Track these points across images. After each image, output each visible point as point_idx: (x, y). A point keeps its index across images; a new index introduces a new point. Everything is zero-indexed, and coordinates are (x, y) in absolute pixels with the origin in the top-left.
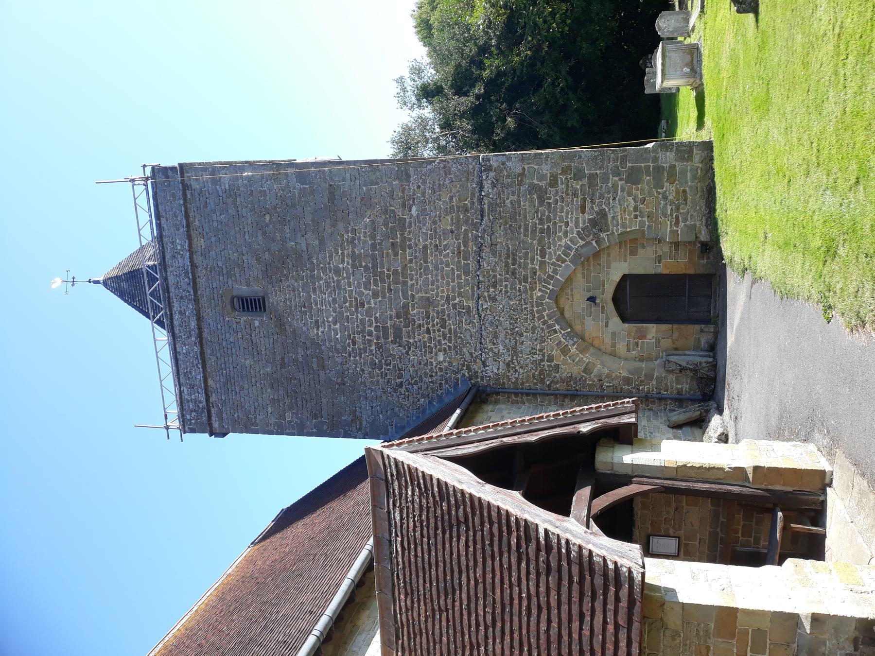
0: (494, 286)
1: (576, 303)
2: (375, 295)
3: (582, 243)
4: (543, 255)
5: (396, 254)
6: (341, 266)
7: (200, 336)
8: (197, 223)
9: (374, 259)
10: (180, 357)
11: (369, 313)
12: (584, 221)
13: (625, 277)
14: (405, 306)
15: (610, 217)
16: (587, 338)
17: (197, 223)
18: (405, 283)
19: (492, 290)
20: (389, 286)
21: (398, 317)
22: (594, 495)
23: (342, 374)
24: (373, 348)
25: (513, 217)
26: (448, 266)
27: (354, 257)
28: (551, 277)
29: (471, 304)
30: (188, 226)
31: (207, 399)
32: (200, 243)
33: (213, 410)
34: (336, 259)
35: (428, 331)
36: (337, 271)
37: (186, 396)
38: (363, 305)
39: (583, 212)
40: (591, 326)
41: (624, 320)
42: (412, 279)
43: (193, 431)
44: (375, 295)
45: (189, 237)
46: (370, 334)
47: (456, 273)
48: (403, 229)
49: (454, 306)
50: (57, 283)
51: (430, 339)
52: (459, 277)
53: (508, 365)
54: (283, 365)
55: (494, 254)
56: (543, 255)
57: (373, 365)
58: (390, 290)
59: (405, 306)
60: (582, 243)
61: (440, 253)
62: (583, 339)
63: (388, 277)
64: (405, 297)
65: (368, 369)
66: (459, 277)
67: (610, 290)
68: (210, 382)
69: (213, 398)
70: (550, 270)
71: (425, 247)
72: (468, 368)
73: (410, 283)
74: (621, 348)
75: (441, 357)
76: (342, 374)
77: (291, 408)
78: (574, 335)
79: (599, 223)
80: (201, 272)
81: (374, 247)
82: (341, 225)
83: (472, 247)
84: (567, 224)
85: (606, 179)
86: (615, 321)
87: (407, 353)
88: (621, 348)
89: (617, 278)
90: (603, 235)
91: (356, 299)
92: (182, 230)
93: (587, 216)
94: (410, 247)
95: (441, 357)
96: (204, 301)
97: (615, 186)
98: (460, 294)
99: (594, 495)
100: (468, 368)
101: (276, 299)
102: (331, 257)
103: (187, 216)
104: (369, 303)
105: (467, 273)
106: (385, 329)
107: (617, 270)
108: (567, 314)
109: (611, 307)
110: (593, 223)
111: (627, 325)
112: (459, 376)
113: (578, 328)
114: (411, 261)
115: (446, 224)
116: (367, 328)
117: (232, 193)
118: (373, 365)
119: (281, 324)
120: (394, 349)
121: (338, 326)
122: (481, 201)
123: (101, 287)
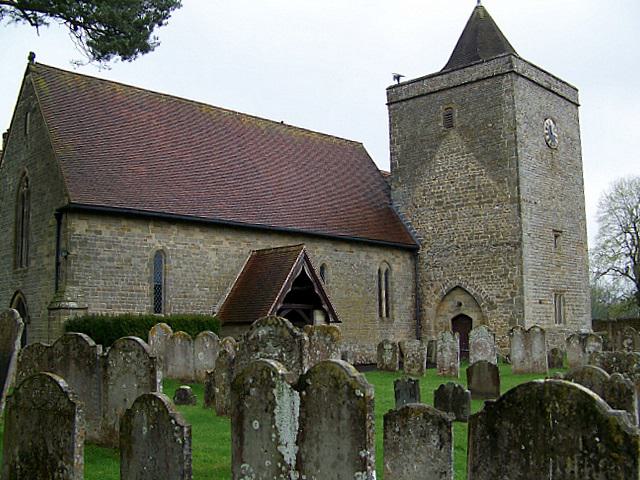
0: (464, 255)
1: (459, 297)
2: (457, 189)
4: (478, 278)
7: (432, 93)
9: (474, 187)
10: (421, 83)
13: (471, 319)
14: (453, 207)
16: (444, 303)
18: (463, 205)
22: (304, 310)
23: (420, 174)
25: (494, 262)
27: (474, 176)
30: (484, 79)
31: (403, 100)
32: (476, 87)
33: (398, 104)
34: (472, 166)
36: (467, 167)
37: (404, 88)
40: (449, 305)
41: (453, 320)
43: (388, 94)
44: (457, 189)
45: (478, 80)
48: (488, 202)
53: (427, 264)
54: (422, 141)
55: (478, 253)
56: (478, 278)
57: (424, 191)
59: (453, 207)
62: (443, 300)
65: (422, 188)
67: (466, 313)
68: (411, 101)
69: (404, 103)
70: (471, 282)
74: (441, 319)
75: (430, 228)
76: (420, 174)
77: (402, 147)
78: (444, 298)
79: (492, 306)
80: (463, 89)
82: (489, 167)
85: (511, 308)
86: (452, 316)
88: (441, 319)
89: (471, 316)
92: (481, 76)
95: (430, 228)
96: (449, 92)
97: (508, 313)
99: (304, 310)
101: (453, 135)
103: (488, 78)
105: (469, 239)
107: (474, 316)
108: (454, 292)
109: (457, 314)
110: (492, 303)
111: (450, 321)
113: (448, 298)
115: (492, 226)
117: (501, 100)
118: (424, 191)
119: (441, 137)
120: (432, 202)
122: (502, 244)
123: (475, 4)
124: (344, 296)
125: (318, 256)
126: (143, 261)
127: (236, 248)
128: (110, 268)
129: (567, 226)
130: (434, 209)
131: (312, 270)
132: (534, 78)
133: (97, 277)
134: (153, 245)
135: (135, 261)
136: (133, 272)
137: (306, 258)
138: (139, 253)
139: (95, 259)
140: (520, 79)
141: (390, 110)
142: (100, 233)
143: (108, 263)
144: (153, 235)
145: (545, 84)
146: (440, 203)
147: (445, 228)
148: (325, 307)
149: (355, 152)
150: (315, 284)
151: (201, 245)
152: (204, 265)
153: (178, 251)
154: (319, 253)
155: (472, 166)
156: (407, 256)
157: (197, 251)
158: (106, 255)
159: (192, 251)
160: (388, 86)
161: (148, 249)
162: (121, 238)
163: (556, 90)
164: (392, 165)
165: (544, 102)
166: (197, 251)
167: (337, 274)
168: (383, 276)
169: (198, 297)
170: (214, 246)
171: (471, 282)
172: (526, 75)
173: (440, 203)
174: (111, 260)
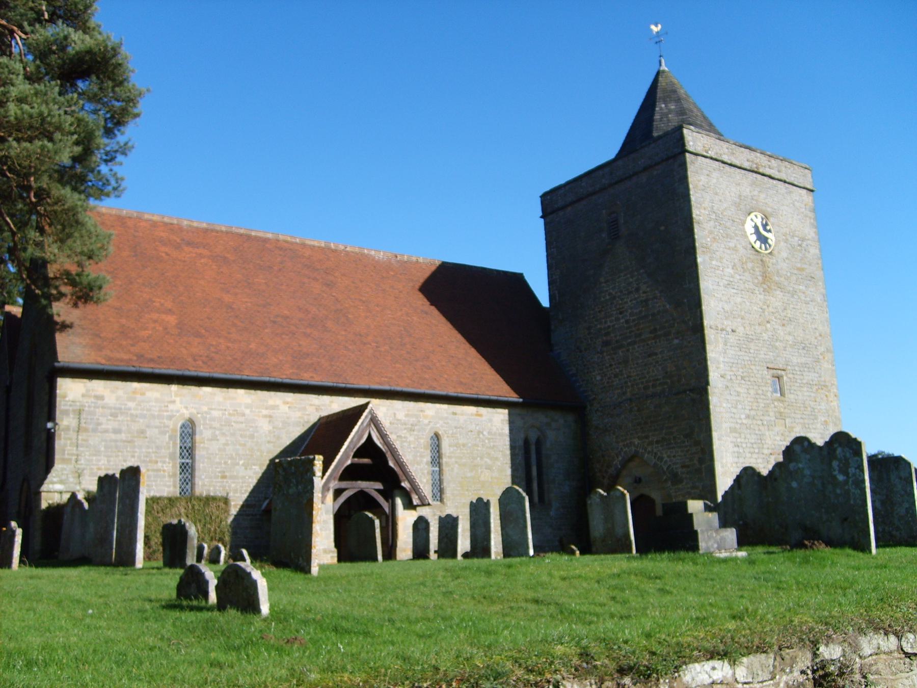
2: (627, 322)
3: (665, 469)
4: (657, 442)
5: (651, 333)
6: (641, 292)
8: (655, 173)
11: (618, 319)
12: (676, 468)
15: (680, 486)
17: (655, 173)
18: (635, 343)
19: (636, 408)
20: (632, 331)
21: (617, 342)
22: (378, 491)
24: (599, 326)
26: (648, 373)
27: (646, 301)
28: (645, 450)
29: (628, 395)
35: (611, 365)
36: (637, 290)
38: (621, 313)
39: (683, 467)
42: (638, 347)
45: (645, 169)
46: (606, 322)
47: (644, 380)
49: (626, 383)
50: (655, 29)
51: (607, 368)
52: (642, 383)
56: (657, 442)
58: (631, 332)
60: (665, 469)
61: (655, 366)
63: (638, 330)
64: (629, 344)
66: (642, 383)
67: (646, 491)
69: (561, 213)
70: (649, 449)
71: (656, 354)
72: (594, 399)
73: (636, 346)
81: (653, 315)
83: (659, 389)
84: (674, 456)
87: (598, 353)
90: (669, 484)
91: (623, 308)
93: (680, 471)
94: (656, 343)
95: (598, 378)
98: (632, 386)
99: (378, 491)
100: (594, 399)
102: (645, 283)
104: (622, 318)
106: (607, 334)
108: (631, 465)
112: (590, 393)
114: (648, 345)
116: (608, 320)
121: (608, 297)
122: (685, 391)
124: (469, 475)
125: (426, 421)
126: (164, 433)
127: (299, 414)
128: (116, 441)
129: (795, 360)
130: (602, 353)
131: (383, 436)
132: (725, 158)
133: (97, 453)
134: (178, 411)
135: (151, 432)
136: (148, 447)
137: (374, 421)
138: (157, 422)
139: (95, 430)
140: (700, 158)
141: (546, 224)
142: (101, 398)
143: (113, 436)
144: (178, 399)
145: (746, 165)
146: (606, 343)
147: (616, 376)
148: (406, 484)
149: (517, 282)
150: (389, 456)
151: (247, 412)
152: (252, 437)
153: (212, 419)
154: (381, 408)
155: (644, 287)
156: (570, 418)
157: (242, 419)
158: (111, 425)
159: (233, 419)
160: (541, 193)
161: (170, 418)
162: (131, 405)
163: (768, 171)
164: (552, 298)
165: (746, 190)
166: (242, 419)
167: (457, 445)
168: (533, 448)
169: (244, 477)
170: (265, 412)
171: (649, 449)
172: (711, 153)
173: (606, 343)
174: (117, 431)
